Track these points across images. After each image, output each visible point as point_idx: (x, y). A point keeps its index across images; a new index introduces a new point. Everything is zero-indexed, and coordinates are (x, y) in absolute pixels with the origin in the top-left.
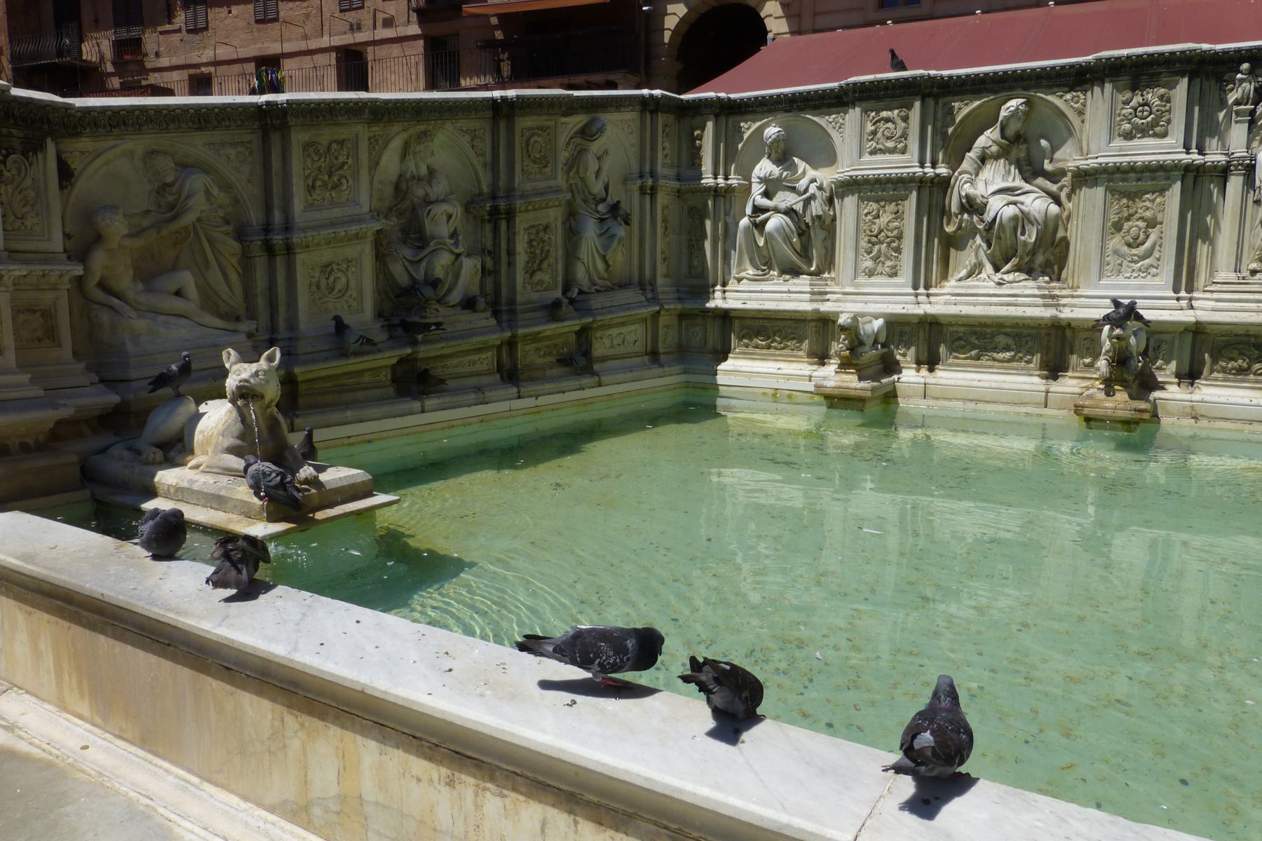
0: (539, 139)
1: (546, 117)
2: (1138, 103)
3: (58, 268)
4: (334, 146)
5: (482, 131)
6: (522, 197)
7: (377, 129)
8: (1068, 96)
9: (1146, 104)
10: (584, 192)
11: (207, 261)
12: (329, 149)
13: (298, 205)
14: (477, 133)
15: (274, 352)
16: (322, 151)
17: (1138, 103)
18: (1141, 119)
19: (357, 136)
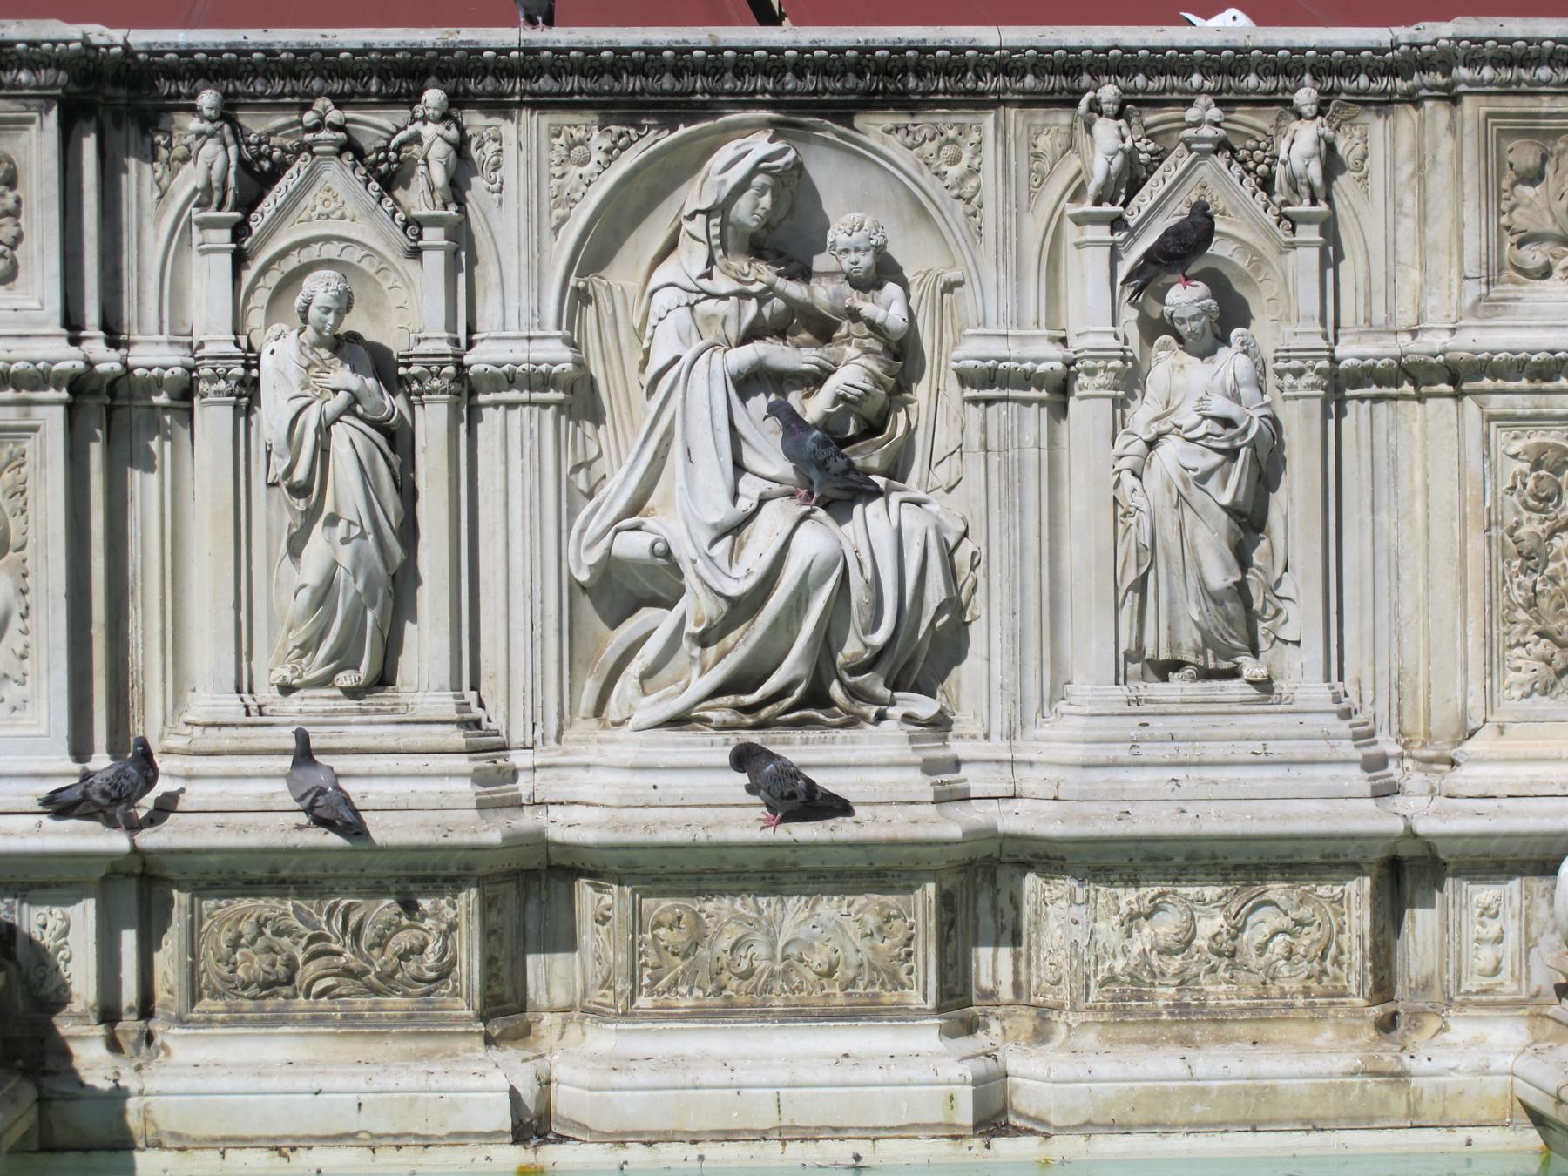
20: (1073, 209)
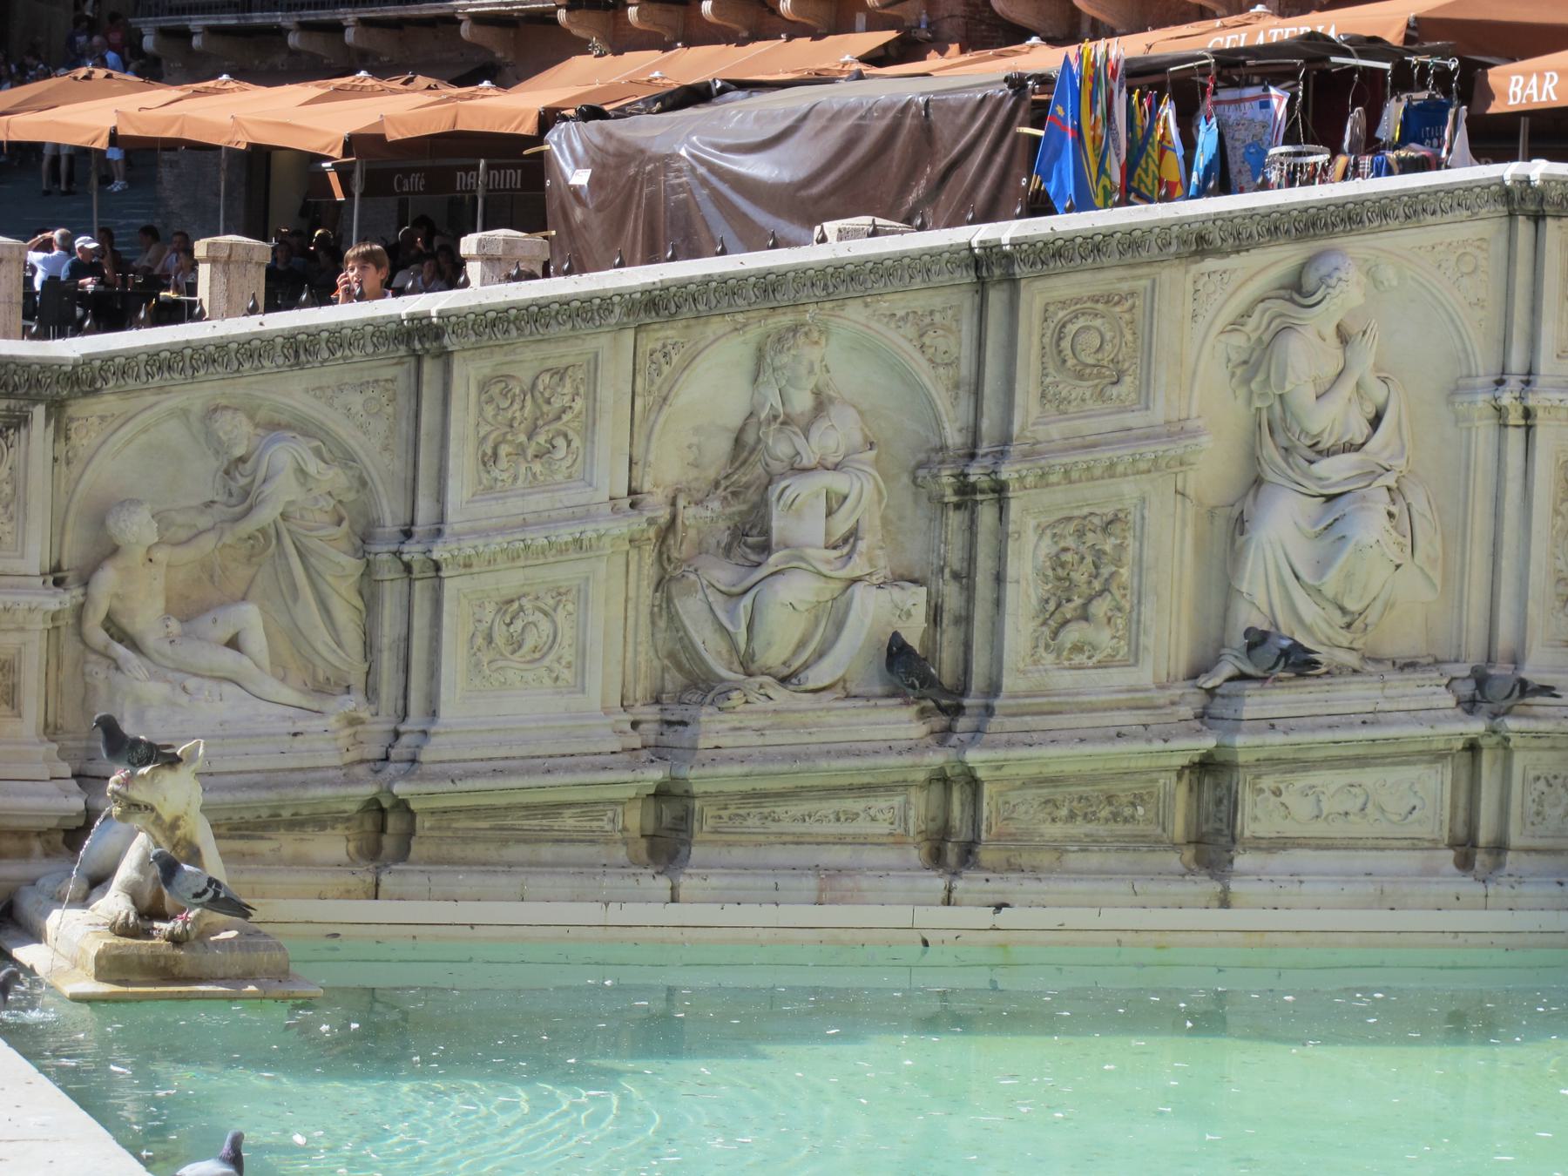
0: (1098, 322)
1: (1122, 272)
3: (24, 600)
4: (546, 378)
5: (950, 313)
6: (1025, 456)
7: (670, 333)
10: (1287, 429)
11: (294, 588)
12: (534, 386)
13: (458, 492)
14: (937, 317)
15: (198, 745)
16: (517, 391)
19: (596, 355)
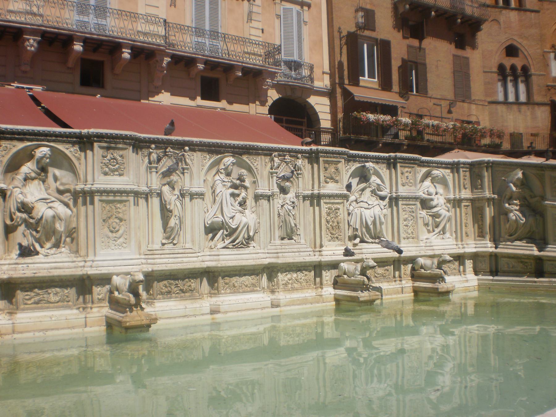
2: (111, 158)
8: (72, 149)
9: (114, 159)
17: (111, 158)
18: (113, 166)
20: (271, 171)
